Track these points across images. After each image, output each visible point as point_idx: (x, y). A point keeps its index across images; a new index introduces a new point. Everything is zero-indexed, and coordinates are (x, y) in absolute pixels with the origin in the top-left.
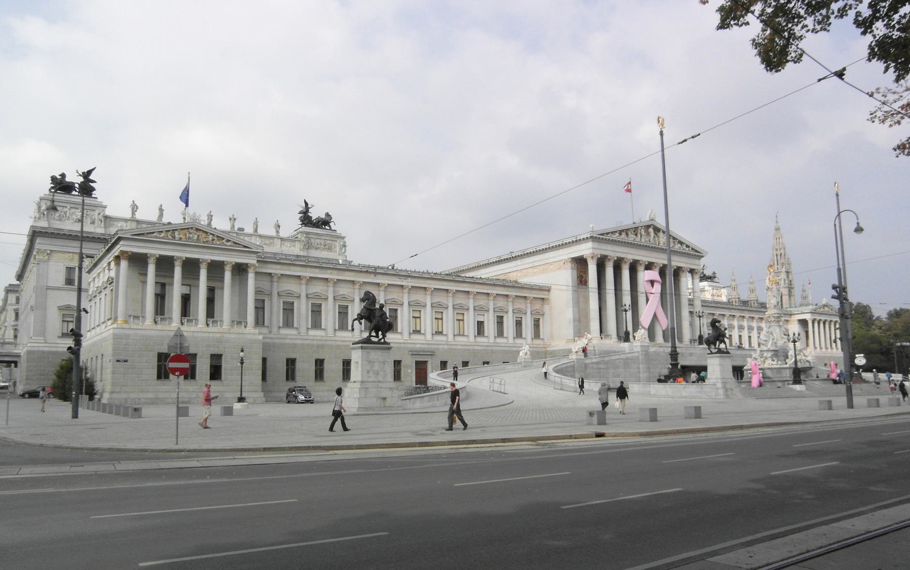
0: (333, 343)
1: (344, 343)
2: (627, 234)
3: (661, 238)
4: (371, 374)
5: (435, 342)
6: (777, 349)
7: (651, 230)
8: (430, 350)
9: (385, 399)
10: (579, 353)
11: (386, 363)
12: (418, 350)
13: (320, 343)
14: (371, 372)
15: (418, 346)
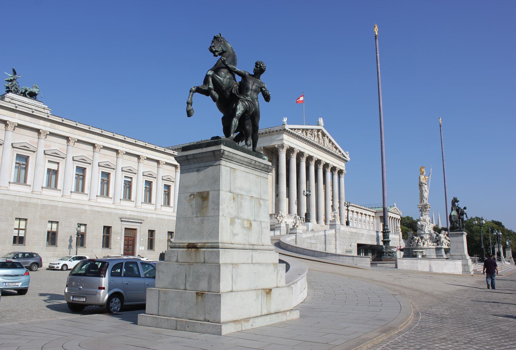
0: (39, 202)
1: (53, 203)
2: (306, 135)
3: (326, 141)
4: (238, 228)
5: (144, 211)
6: (429, 233)
7: (320, 133)
8: (140, 218)
9: (269, 291)
10: (299, 228)
11: (262, 202)
12: (128, 217)
13: (23, 200)
14: (237, 221)
15: (128, 213)
